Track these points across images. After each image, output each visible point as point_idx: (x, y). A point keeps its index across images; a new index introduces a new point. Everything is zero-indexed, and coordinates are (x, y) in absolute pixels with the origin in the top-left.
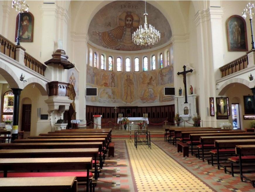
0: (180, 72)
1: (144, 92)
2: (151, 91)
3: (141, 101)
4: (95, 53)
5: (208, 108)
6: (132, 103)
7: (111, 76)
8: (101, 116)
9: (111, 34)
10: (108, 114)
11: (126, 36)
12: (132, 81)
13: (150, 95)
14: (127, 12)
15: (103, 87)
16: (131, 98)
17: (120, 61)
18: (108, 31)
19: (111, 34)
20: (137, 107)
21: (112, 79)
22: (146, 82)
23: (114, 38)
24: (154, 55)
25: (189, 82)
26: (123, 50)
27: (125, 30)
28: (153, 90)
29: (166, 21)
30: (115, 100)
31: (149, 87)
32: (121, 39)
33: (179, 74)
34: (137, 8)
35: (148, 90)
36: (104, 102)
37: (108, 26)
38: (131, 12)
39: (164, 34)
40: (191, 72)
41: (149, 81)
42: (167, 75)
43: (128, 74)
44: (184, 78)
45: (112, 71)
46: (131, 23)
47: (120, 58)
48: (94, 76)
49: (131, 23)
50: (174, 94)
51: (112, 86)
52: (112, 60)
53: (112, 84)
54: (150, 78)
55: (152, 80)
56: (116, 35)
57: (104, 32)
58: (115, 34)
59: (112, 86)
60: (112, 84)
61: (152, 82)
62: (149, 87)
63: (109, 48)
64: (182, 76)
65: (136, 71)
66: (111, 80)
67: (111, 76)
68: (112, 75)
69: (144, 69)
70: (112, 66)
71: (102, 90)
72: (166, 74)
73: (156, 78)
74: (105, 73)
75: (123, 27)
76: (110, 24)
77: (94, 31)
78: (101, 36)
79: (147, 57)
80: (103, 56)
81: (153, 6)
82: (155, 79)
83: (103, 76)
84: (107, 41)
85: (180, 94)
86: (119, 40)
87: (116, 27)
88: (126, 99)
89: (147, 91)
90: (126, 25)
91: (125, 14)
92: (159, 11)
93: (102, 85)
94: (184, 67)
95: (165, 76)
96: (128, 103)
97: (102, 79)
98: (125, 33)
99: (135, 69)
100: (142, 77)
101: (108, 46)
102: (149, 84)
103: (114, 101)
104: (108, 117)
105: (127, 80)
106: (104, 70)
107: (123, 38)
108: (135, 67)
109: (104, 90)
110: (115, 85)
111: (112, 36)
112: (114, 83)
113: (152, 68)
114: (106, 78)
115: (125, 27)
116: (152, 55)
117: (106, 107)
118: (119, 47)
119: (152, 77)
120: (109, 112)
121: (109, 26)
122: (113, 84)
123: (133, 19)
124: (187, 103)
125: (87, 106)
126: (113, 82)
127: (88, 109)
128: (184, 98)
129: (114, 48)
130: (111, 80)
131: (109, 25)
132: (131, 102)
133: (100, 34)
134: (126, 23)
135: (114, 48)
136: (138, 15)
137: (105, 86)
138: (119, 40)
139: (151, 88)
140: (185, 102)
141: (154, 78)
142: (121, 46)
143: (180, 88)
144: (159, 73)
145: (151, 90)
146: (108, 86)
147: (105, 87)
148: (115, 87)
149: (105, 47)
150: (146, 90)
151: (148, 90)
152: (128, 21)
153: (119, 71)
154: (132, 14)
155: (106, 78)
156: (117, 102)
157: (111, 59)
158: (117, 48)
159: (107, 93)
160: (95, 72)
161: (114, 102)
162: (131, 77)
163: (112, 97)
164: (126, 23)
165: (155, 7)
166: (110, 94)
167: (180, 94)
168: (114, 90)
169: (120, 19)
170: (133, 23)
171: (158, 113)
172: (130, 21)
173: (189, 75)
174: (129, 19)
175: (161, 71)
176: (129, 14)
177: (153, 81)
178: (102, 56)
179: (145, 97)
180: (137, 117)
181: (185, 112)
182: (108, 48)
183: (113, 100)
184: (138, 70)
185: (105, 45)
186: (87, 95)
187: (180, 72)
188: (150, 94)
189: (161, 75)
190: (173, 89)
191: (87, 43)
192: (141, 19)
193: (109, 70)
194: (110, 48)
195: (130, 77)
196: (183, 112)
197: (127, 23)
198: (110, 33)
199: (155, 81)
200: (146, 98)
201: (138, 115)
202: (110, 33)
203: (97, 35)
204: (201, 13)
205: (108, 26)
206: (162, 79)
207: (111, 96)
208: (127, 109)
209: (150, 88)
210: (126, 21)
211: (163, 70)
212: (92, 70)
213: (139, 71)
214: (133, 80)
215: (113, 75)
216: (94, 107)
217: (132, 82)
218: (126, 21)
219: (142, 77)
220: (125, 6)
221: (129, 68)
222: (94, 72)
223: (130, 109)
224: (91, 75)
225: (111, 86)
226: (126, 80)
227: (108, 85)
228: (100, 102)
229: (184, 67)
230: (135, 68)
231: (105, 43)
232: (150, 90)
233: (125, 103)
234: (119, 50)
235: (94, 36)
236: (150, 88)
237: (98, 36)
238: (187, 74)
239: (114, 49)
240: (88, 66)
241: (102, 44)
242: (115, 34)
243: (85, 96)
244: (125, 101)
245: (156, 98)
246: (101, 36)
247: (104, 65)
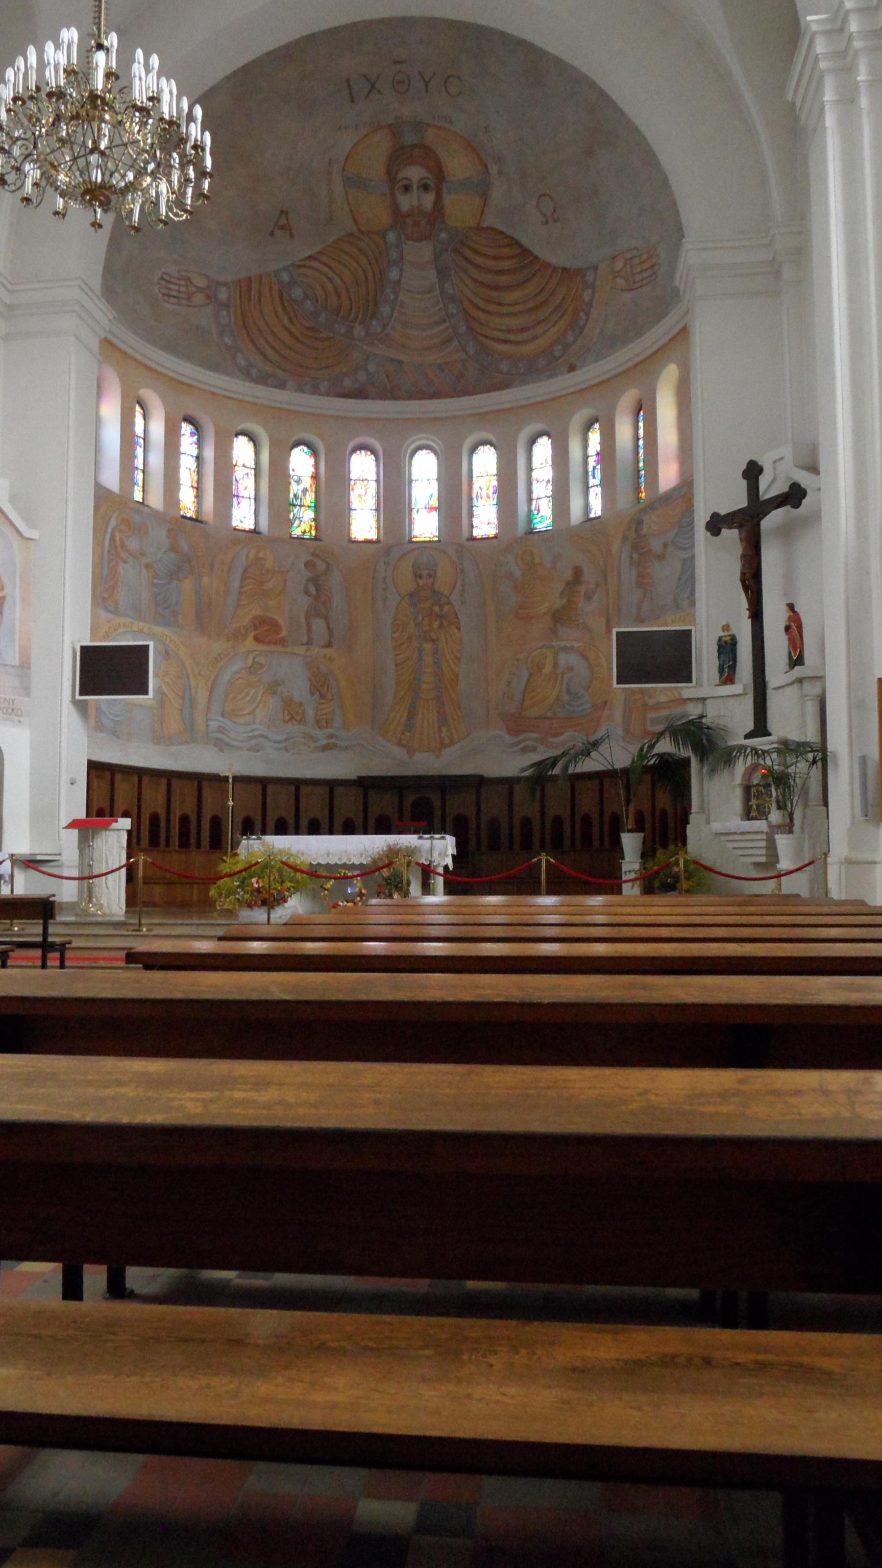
0: (724, 510)
1: (525, 675)
2: (570, 669)
3: (508, 739)
4: (189, 420)
5: (863, 759)
6: (446, 751)
7: (306, 574)
8: (125, 823)
9: (298, 293)
10: (184, 820)
11: (402, 296)
12: (449, 603)
13: (566, 697)
14: (395, 130)
15: (249, 643)
16: (443, 720)
17: (374, 477)
18: (276, 273)
19: (298, 293)
20: (479, 782)
21: (313, 590)
22: (544, 607)
23: (322, 318)
24: (597, 421)
25: (789, 578)
26: (391, 393)
27: (394, 255)
28: (587, 659)
29: (650, 159)
30: (331, 736)
31: (555, 644)
32: (374, 315)
33: (716, 525)
34: (453, 90)
35: (555, 665)
36: (254, 742)
37: (272, 234)
38: (419, 126)
39: (650, 257)
40: (797, 505)
41: (564, 601)
42: (671, 549)
43: (424, 559)
44: (743, 557)
45: (316, 538)
46: (428, 200)
47: (373, 452)
48: (174, 574)
49: (428, 200)
50: (689, 679)
51: (309, 643)
52: (316, 466)
53: (309, 630)
54: (568, 575)
55: (582, 589)
56: (338, 294)
57: (249, 280)
58: (330, 287)
59: (309, 643)
60: (309, 630)
61: (581, 603)
62: (555, 644)
63: (290, 384)
64: (731, 535)
65: (477, 533)
66: (306, 601)
67: (306, 574)
68: (308, 565)
69: (530, 521)
70: (317, 508)
71: (237, 666)
72: (665, 546)
73: (604, 574)
74: (261, 555)
75: (383, 234)
76: (283, 221)
77: (172, 269)
78: (227, 306)
79: (549, 436)
80: (142, 408)
81: (558, 61)
82: (598, 585)
83: (245, 571)
84: (274, 335)
85: (728, 674)
86: (359, 331)
87: (331, 240)
88: (409, 726)
89: (547, 670)
90: (398, 217)
91: (382, 144)
92: (602, 94)
93: (237, 636)
94: (753, 472)
95: (661, 557)
96: (419, 756)
97: (241, 593)
98: (394, 274)
99: (475, 522)
100: (518, 573)
101: (280, 373)
102: (559, 617)
103: (324, 742)
104: (184, 843)
105: (413, 597)
106: (255, 532)
107: (385, 310)
108: (471, 507)
109: (255, 667)
110: (330, 630)
111: (308, 304)
112: (327, 620)
113: (587, 508)
114: (269, 585)
115: (392, 237)
116: (586, 412)
117: (298, 784)
118: (362, 377)
119: (578, 573)
120: (189, 807)
121: (278, 233)
122: (319, 625)
123: (439, 173)
124: (770, 735)
125: (95, 768)
126: (319, 615)
127: (102, 787)
128: (748, 703)
129: (324, 386)
130: (305, 602)
131: (282, 228)
132: (443, 745)
133: (223, 295)
134: (395, 209)
135: (324, 386)
136: (471, 147)
137: (256, 639)
138: (359, 331)
139: (572, 648)
140: (750, 726)
141: (590, 577)
142: (372, 367)
143: (726, 628)
144: (625, 538)
145: (574, 660)
146: (283, 642)
147: (260, 647)
148: (329, 645)
149: (262, 380)
150: (540, 667)
151: (555, 665)
152: (407, 189)
153: (367, 542)
154: (431, 137)
155: (269, 585)
156: (347, 748)
157: (312, 461)
158: (347, 383)
159: (273, 688)
160: (184, 546)
161: (325, 748)
162: (439, 574)
163: (310, 712)
164: (395, 209)
165: (576, 70)
166: (297, 696)
167: (721, 670)
168: (323, 669)
169: (354, 182)
170: (447, 200)
171: (587, 819)
172: (426, 188)
173: (788, 532)
174: (414, 173)
175: (640, 523)
176: (410, 139)
177: (589, 597)
178: (186, 428)
179: (533, 712)
180: (365, 832)
181: (753, 802)
182: (281, 385)
183: (317, 733)
184: (491, 531)
185: (269, 368)
186: (82, 693)
187: (723, 512)
188: (569, 692)
189: (635, 556)
190: (683, 639)
191: (95, 345)
192: (493, 169)
193: (296, 532)
194: (300, 389)
195: (432, 575)
196: (737, 804)
197: (405, 202)
198: (292, 283)
199: (596, 596)
200: (540, 718)
201: (371, 823)
202: (292, 283)
203: (199, 298)
204: (827, 33)
205: (272, 234)
206: (642, 581)
207: (301, 705)
208: (410, 799)
209: (565, 649)
210: (393, 194)
211: (646, 518)
212: (160, 534)
213: (496, 537)
214: (455, 598)
215: (321, 566)
216: (169, 777)
217: (446, 609)
218: (393, 194)
219: (518, 573)
220: (373, 86)
221: (435, 515)
222: (174, 549)
223: (435, 798)
224: (147, 566)
225: (305, 639)
226: (411, 595)
227: (284, 633)
228: (221, 745)
229: (753, 472)
230: (471, 515)
231: (264, 355)
232: (563, 659)
233: (399, 752)
234: (360, 394)
235: (167, 305)
236: (565, 649)
237: (209, 310)
238: (771, 521)
239: (328, 394)
240: (102, 495)
241: (239, 356)
242: (330, 287)
243: (74, 702)
244: (400, 744)
245: (605, 713)
246: (227, 306)
247: (256, 499)
